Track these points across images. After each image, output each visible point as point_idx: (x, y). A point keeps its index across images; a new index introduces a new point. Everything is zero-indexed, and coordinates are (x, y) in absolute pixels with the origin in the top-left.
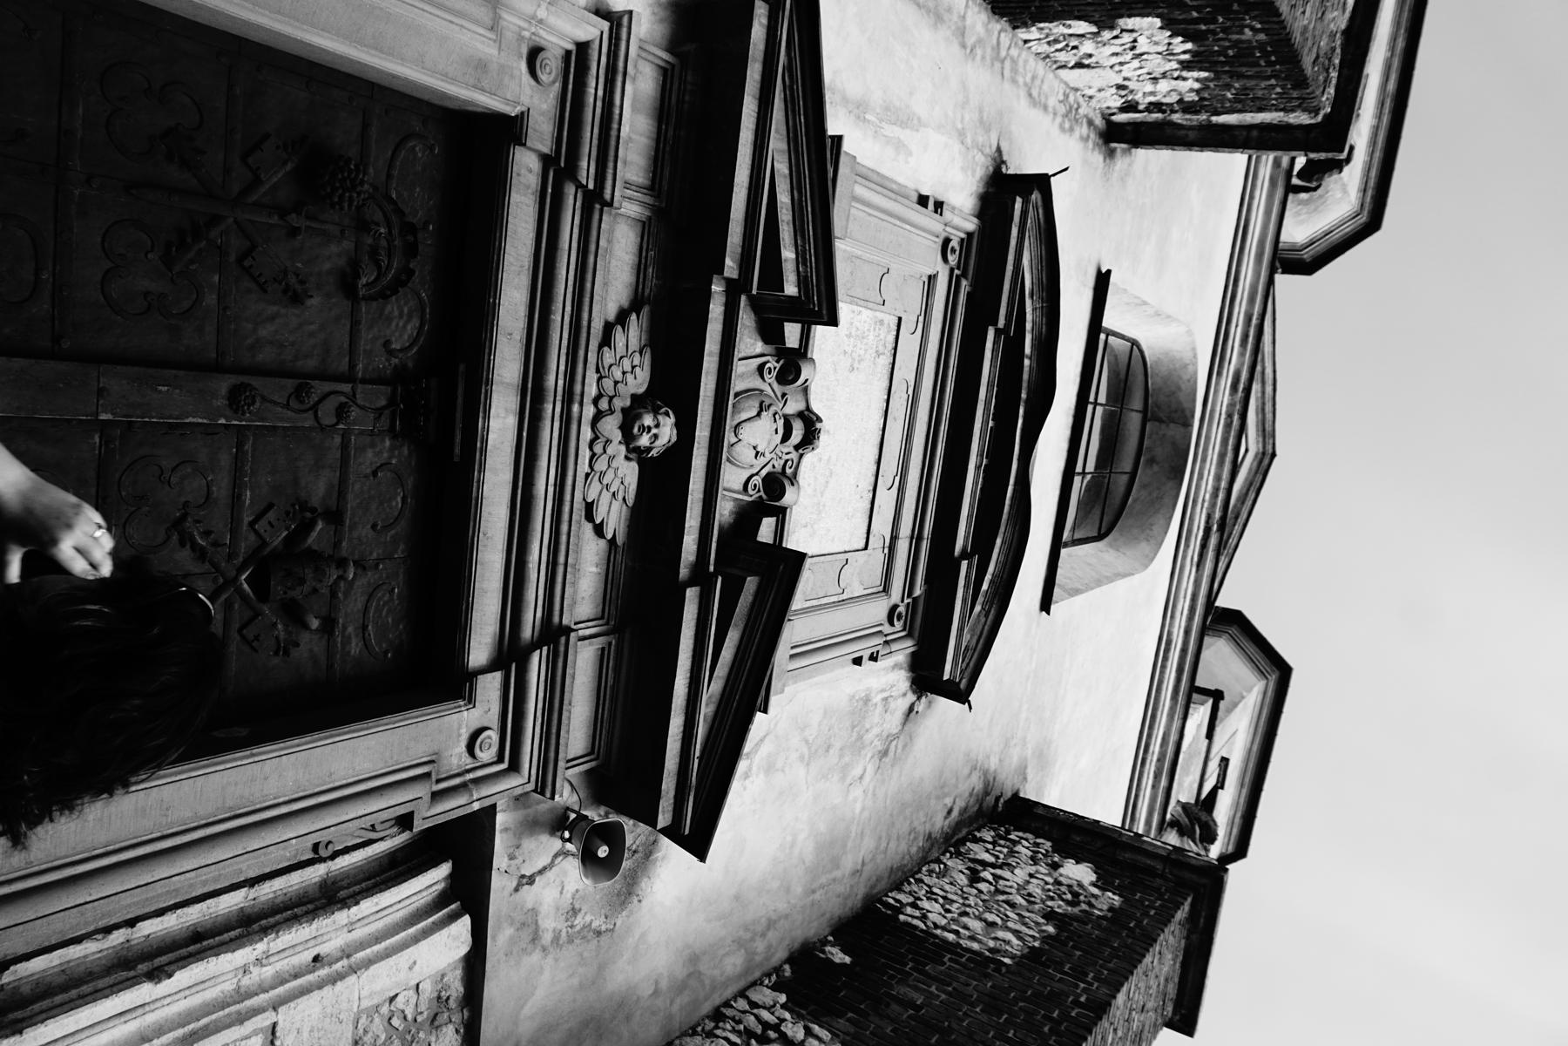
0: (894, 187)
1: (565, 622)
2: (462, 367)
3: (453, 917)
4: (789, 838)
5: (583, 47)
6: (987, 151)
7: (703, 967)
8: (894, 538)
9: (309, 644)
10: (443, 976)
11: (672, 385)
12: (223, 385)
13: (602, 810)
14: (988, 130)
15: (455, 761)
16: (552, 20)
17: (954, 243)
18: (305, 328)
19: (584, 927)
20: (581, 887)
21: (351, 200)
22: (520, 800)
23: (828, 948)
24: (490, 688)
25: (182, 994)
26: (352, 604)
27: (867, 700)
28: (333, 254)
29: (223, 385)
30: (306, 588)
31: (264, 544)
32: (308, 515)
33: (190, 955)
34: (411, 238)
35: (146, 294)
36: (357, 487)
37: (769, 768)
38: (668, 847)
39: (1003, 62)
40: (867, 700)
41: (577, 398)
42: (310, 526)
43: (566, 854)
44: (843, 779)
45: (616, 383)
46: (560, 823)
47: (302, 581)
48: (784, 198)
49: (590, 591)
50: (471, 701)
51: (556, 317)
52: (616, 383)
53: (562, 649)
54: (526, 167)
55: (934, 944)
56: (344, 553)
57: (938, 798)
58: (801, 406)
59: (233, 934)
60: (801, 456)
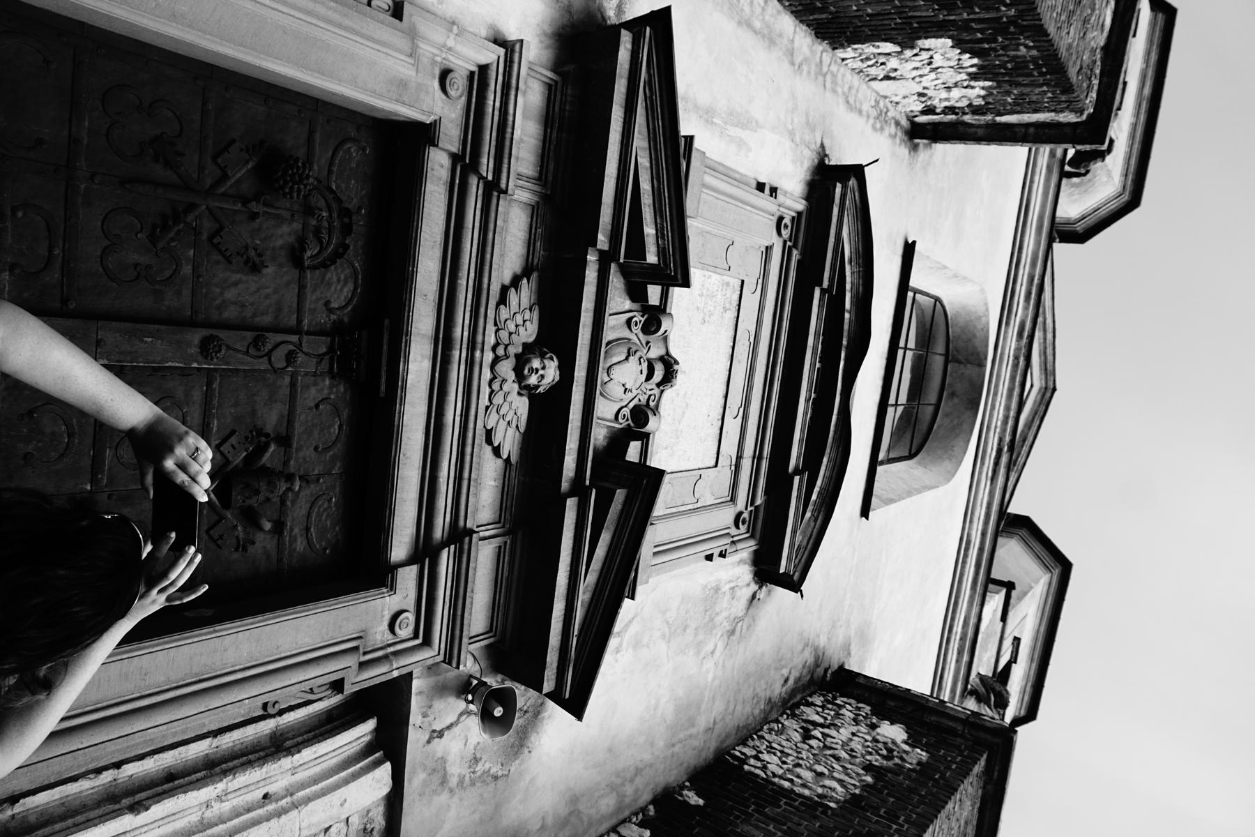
0: (737, 176)
1: (469, 525)
2: (387, 322)
3: (377, 764)
4: (653, 702)
5: (484, 69)
6: (813, 147)
7: (581, 807)
8: (739, 457)
9: (263, 542)
10: (368, 811)
11: (556, 335)
12: (196, 336)
13: (499, 677)
14: (813, 130)
15: (379, 637)
16: (459, 48)
17: (787, 221)
18: (262, 291)
19: (484, 772)
20: (481, 740)
21: (299, 191)
22: (432, 669)
23: (685, 792)
24: (408, 578)
25: (156, 824)
26: (297, 512)
27: (717, 589)
28: (285, 233)
29: (196, 336)
30: (261, 497)
31: (228, 462)
32: (263, 439)
33: (165, 792)
34: (346, 220)
35: (136, 265)
36: (303, 417)
37: (637, 644)
38: (553, 708)
39: (825, 76)
40: (717, 589)
41: (479, 346)
42: (267, 446)
43: (470, 713)
44: (698, 653)
45: (510, 334)
46: (465, 688)
47: (257, 492)
48: (646, 186)
49: (490, 501)
50: (393, 588)
52: (510, 334)
53: (466, 547)
54: (438, 163)
55: (772, 790)
56: (292, 470)
57: (776, 669)
58: (662, 352)
59: (199, 775)
60: (662, 392)
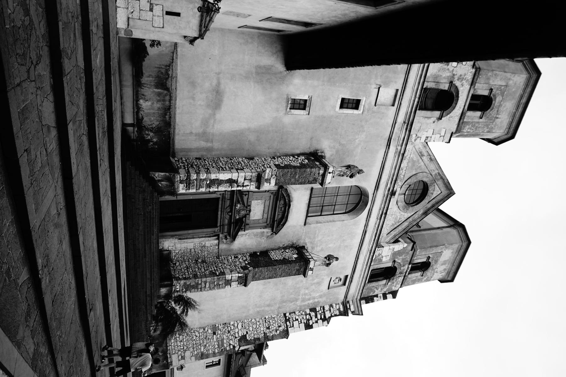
24: (219, 228)
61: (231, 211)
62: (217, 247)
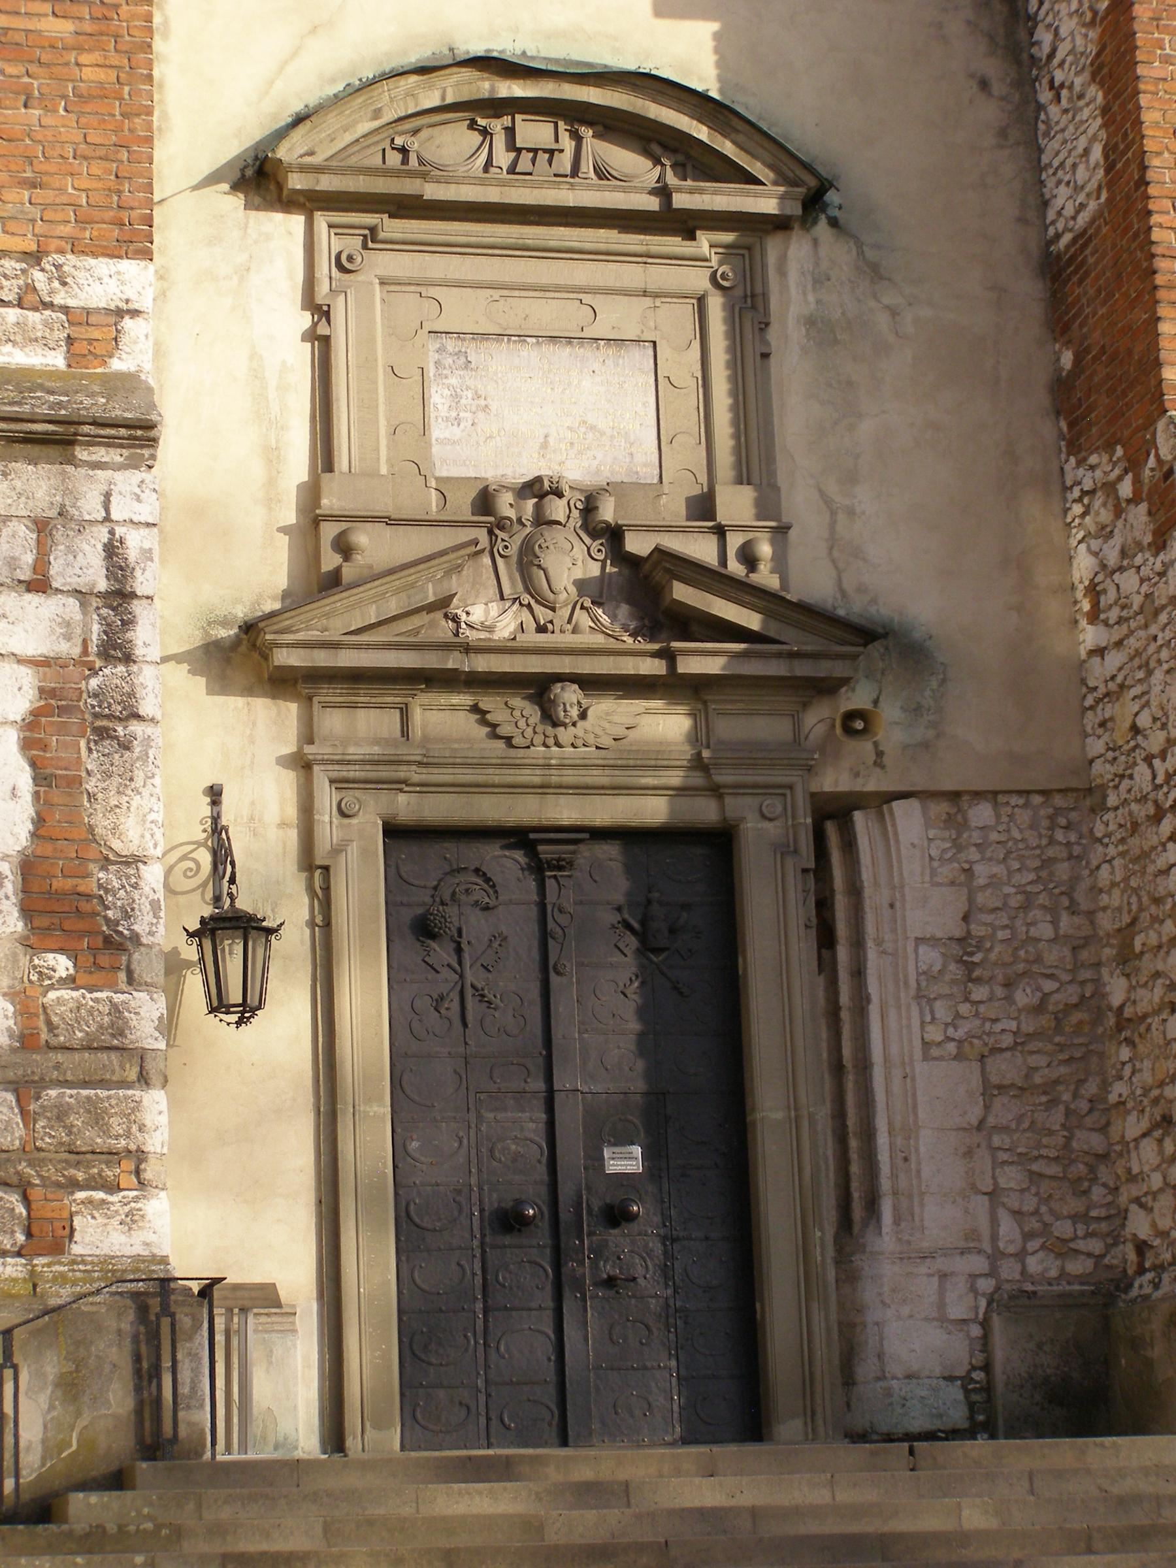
37: (850, 479)
41: (547, 762)
51: (497, 779)
61: (539, 688)
62: (981, 814)
